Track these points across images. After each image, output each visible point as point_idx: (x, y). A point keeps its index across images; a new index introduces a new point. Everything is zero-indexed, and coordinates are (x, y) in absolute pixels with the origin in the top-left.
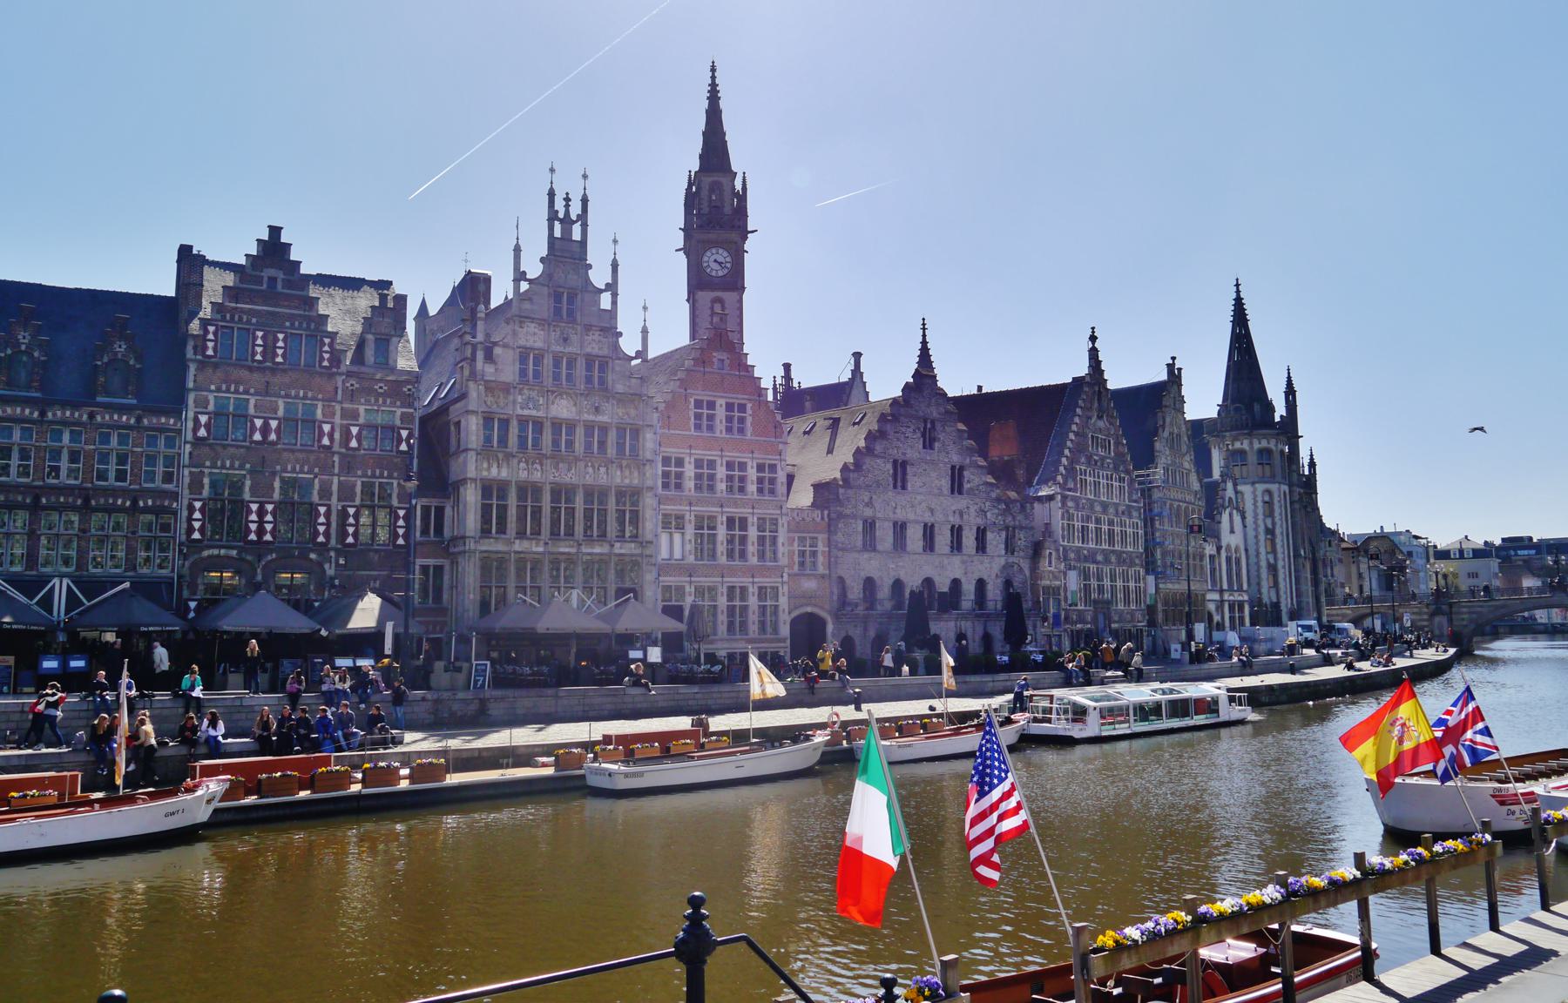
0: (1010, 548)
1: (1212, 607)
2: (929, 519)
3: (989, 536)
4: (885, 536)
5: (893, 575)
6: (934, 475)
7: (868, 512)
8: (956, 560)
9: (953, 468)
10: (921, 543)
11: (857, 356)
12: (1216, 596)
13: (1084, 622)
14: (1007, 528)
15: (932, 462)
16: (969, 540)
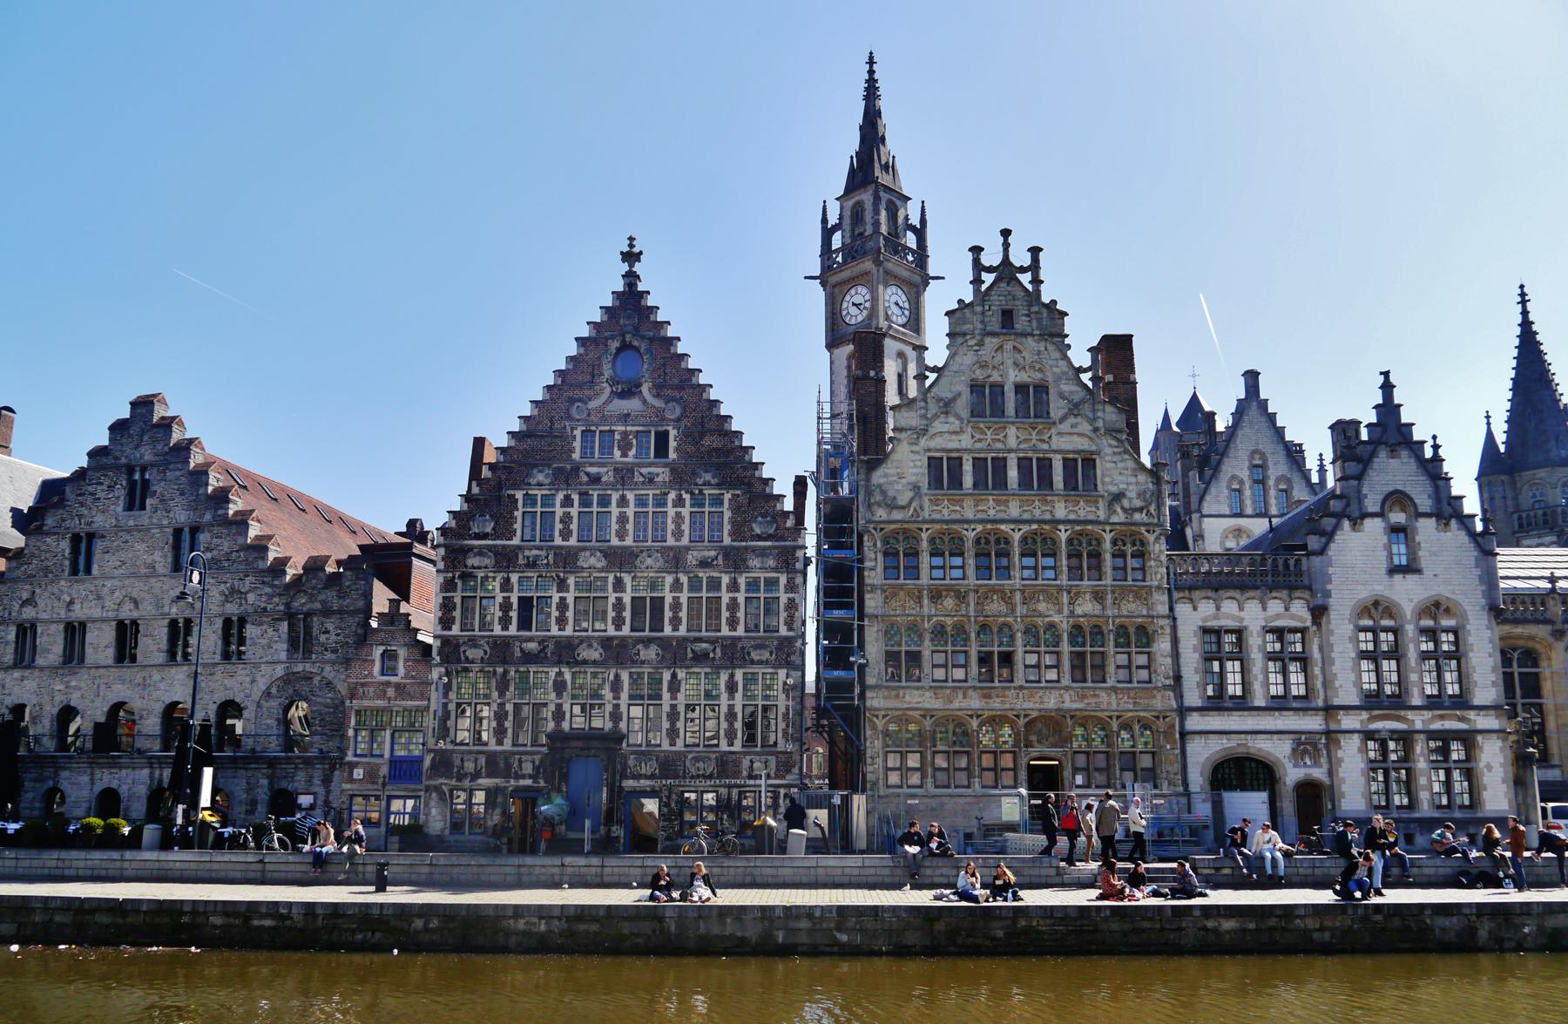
0: (301, 642)
1: (1278, 750)
2: (127, 613)
3: (250, 631)
4: (51, 645)
5: (60, 699)
6: (141, 547)
7: (29, 613)
8: (180, 674)
9: (178, 533)
10: (110, 653)
11: (1252, 378)
12: (1314, 723)
13: (507, 773)
14: (290, 616)
15: (138, 528)
16: (208, 640)
